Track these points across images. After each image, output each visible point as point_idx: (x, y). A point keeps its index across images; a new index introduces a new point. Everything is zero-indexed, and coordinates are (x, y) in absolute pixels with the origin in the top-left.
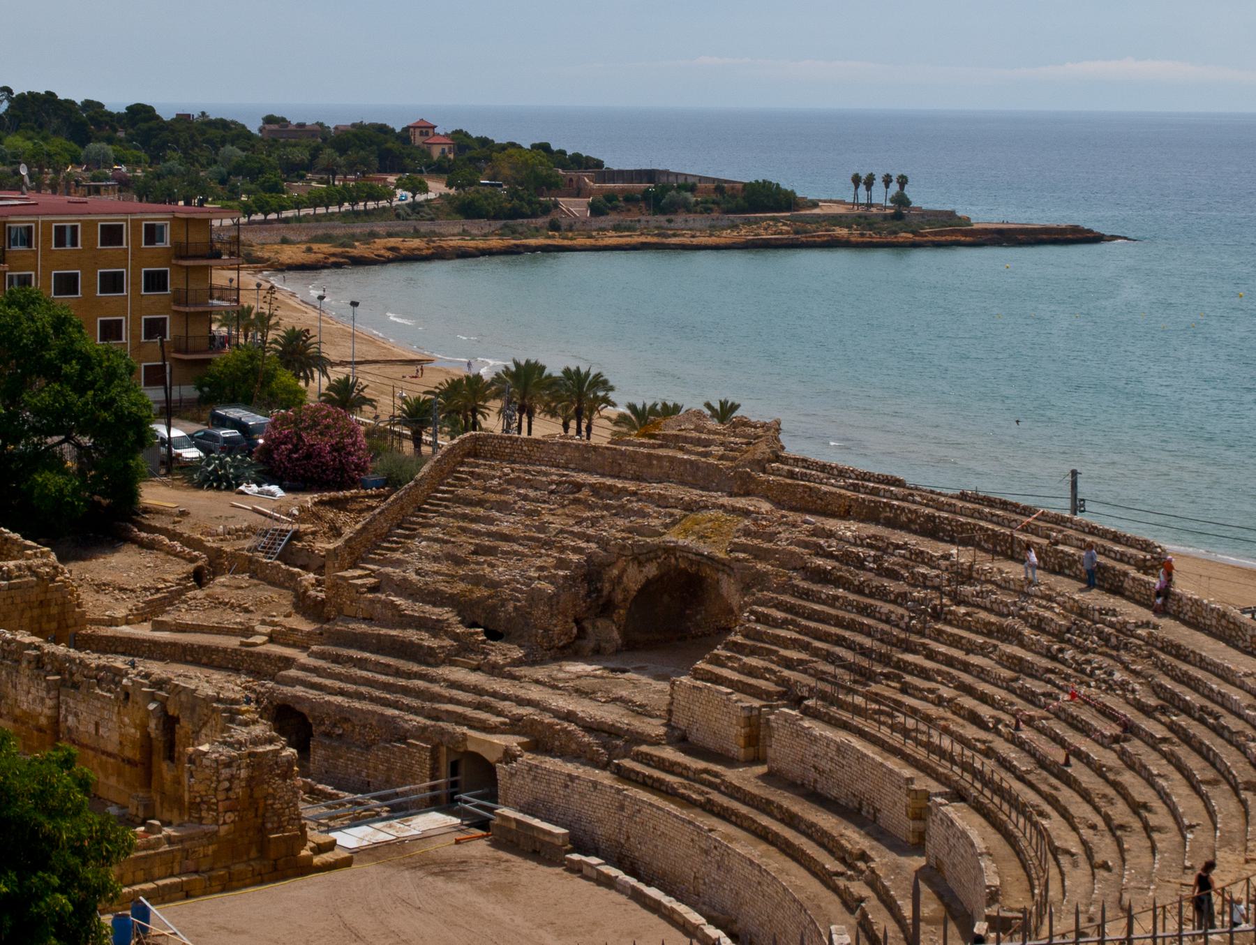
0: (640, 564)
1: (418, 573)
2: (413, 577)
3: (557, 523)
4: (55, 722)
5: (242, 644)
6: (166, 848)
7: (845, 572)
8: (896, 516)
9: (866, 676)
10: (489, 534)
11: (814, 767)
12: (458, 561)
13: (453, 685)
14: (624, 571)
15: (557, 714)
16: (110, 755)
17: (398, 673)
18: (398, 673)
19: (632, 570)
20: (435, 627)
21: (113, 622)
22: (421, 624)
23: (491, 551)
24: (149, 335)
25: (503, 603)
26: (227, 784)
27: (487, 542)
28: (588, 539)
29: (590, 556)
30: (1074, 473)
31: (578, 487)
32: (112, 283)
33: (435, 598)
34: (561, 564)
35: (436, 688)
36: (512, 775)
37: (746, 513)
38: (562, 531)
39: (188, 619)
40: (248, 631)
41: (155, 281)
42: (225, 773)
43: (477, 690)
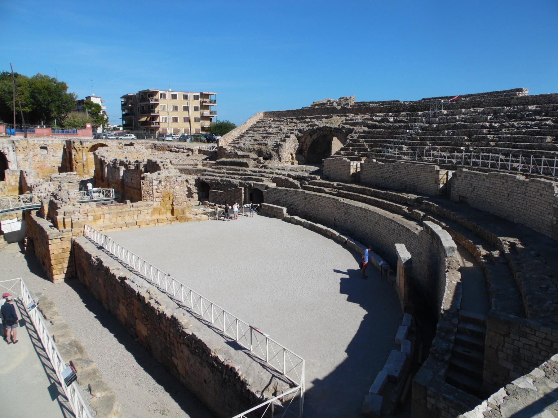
0: (311, 136)
1: (244, 144)
2: (243, 145)
7: (383, 124)
8: (399, 109)
10: (266, 133)
11: (382, 177)
12: (255, 140)
14: (306, 138)
15: (284, 175)
16: (135, 188)
17: (236, 170)
18: (236, 170)
22: (244, 157)
23: (267, 137)
27: (264, 135)
28: (296, 130)
33: (250, 150)
35: (246, 172)
36: (268, 193)
43: (259, 172)
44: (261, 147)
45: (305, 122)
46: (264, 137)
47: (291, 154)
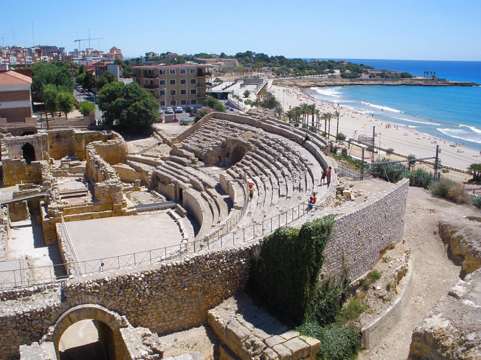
2: (189, 145)
3: (220, 133)
4: (97, 176)
5: (155, 160)
6: (87, 206)
9: (257, 174)
12: (199, 142)
13: (186, 171)
19: (232, 145)
20: (188, 157)
21: (134, 154)
24: (192, 93)
25: (203, 152)
26: (103, 192)
27: (206, 138)
29: (223, 142)
30: (374, 127)
31: (228, 125)
32: (183, 82)
33: (191, 151)
34: (217, 144)
37: (254, 132)
38: (220, 136)
39: (148, 154)
40: (157, 157)
41: (193, 82)
42: (102, 190)
44: (200, 149)
45: (234, 131)
46: (205, 140)
47: (220, 158)
